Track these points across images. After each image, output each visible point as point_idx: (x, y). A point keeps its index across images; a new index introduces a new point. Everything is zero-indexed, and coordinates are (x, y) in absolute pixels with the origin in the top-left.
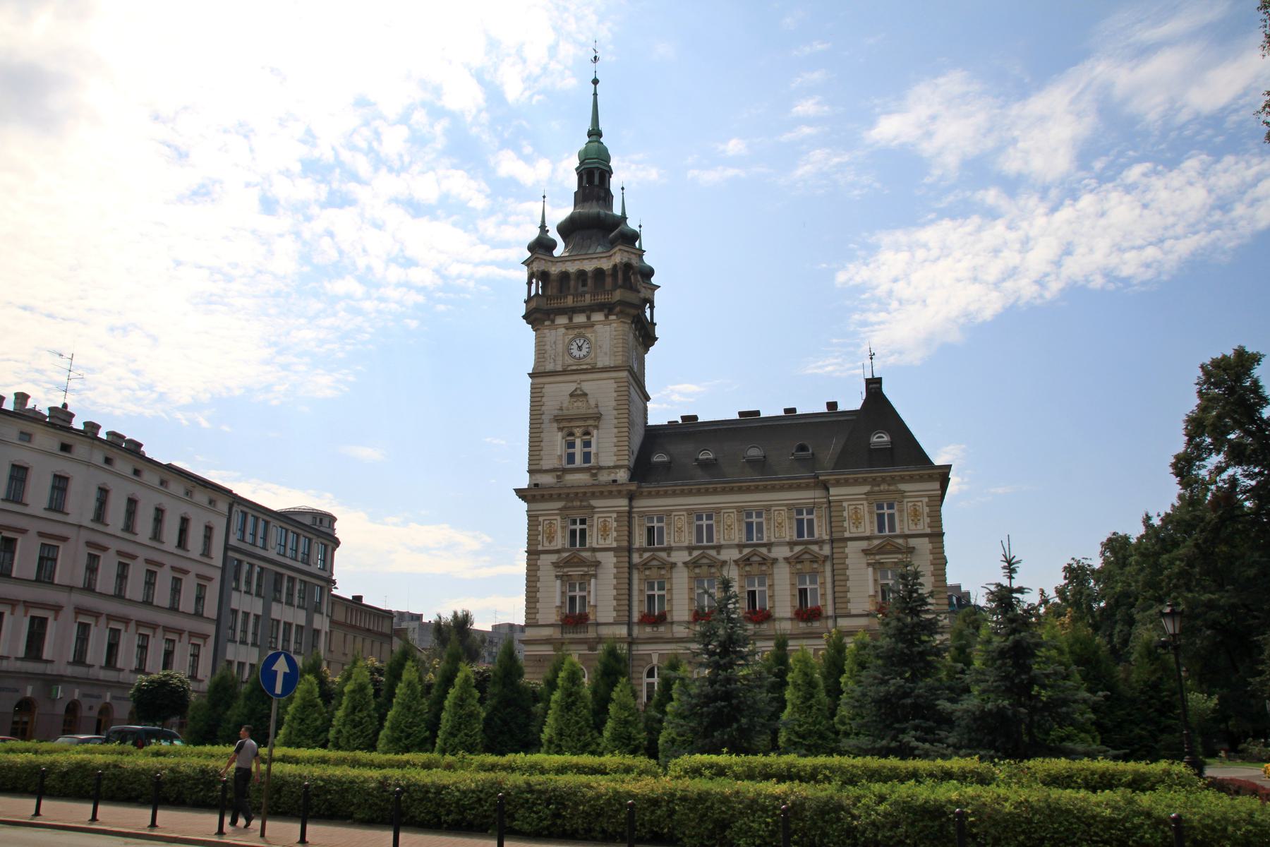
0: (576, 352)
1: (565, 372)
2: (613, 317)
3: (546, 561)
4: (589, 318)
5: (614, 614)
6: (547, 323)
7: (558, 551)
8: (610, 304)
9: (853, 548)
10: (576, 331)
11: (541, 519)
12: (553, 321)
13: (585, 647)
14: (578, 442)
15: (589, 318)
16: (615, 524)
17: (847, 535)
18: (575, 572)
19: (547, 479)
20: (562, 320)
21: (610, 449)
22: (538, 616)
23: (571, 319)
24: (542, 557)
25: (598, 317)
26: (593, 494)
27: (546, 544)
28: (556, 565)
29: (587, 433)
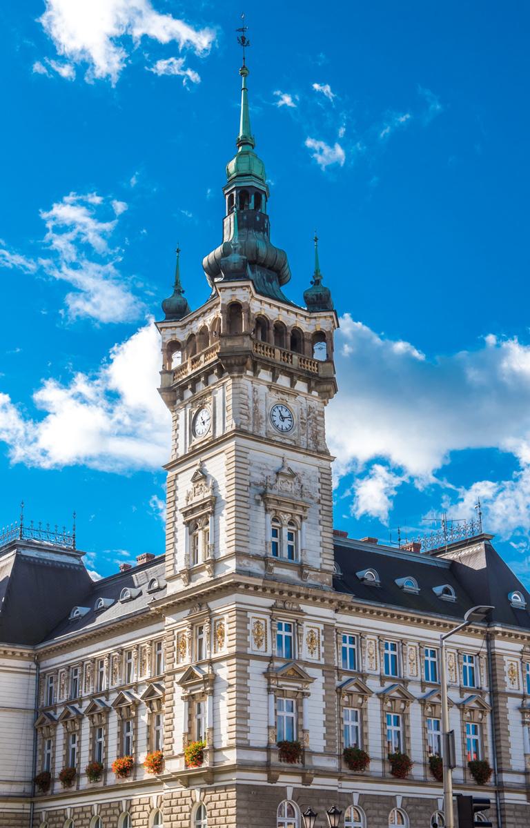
0: (278, 422)
1: (269, 441)
2: (315, 393)
3: (256, 667)
4: (293, 384)
5: (324, 743)
6: (249, 373)
7: (271, 659)
8: (317, 375)
9: (513, 703)
10: (280, 396)
11: (250, 615)
12: (256, 372)
13: (298, 779)
14: (285, 531)
15: (293, 384)
16: (322, 638)
17: (507, 690)
18: (291, 686)
19: (256, 567)
20: (265, 375)
21: (315, 549)
22: (249, 736)
23: (275, 378)
24: (252, 662)
25: (301, 386)
26: (307, 597)
27: (255, 648)
28: (267, 674)
29: (290, 524)
